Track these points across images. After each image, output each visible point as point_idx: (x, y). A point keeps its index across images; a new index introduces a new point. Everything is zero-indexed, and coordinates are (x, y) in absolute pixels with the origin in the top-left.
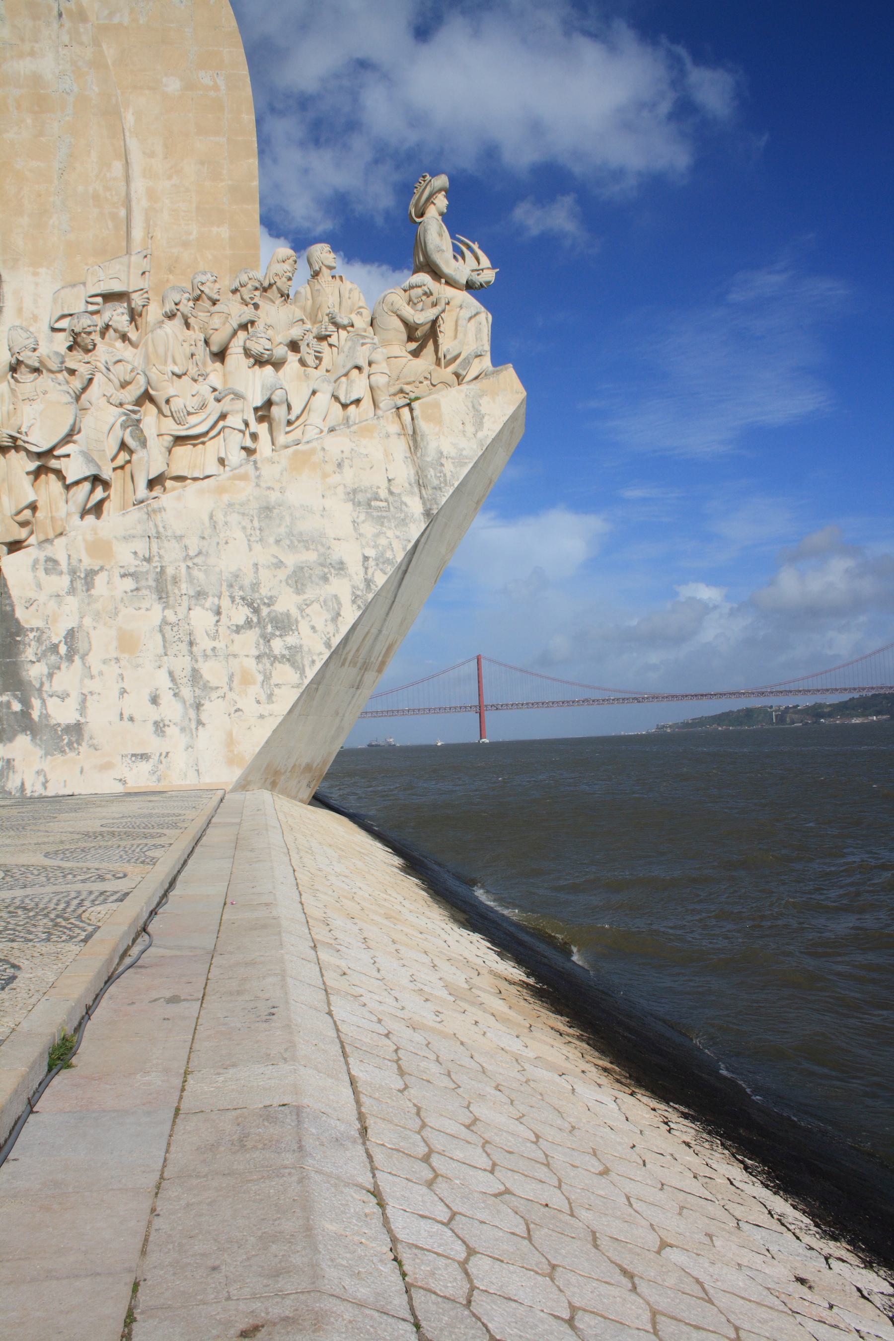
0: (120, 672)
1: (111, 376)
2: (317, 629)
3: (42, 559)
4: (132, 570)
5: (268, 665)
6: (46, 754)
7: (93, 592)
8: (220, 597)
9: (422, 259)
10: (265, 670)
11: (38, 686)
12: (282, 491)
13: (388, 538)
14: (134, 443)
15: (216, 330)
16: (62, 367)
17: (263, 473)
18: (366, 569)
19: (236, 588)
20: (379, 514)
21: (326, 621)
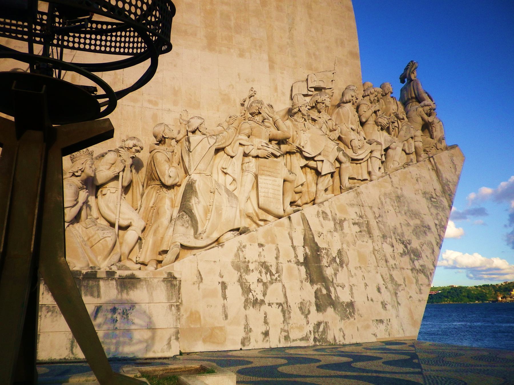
0: (362, 274)
1: (327, 126)
2: (428, 257)
3: (321, 212)
4: (357, 221)
5: (416, 274)
6: (342, 319)
7: (344, 231)
8: (391, 238)
9: (414, 95)
10: (415, 276)
11: (331, 280)
12: (401, 189)
13: (441, 216)
14: (345, 159)
15: (365, 112)
16: (309, 118)
17: (393, 180)
18: (437, 229)
19: (396, 234)
20: (435, 204)
21: (430, 254)
